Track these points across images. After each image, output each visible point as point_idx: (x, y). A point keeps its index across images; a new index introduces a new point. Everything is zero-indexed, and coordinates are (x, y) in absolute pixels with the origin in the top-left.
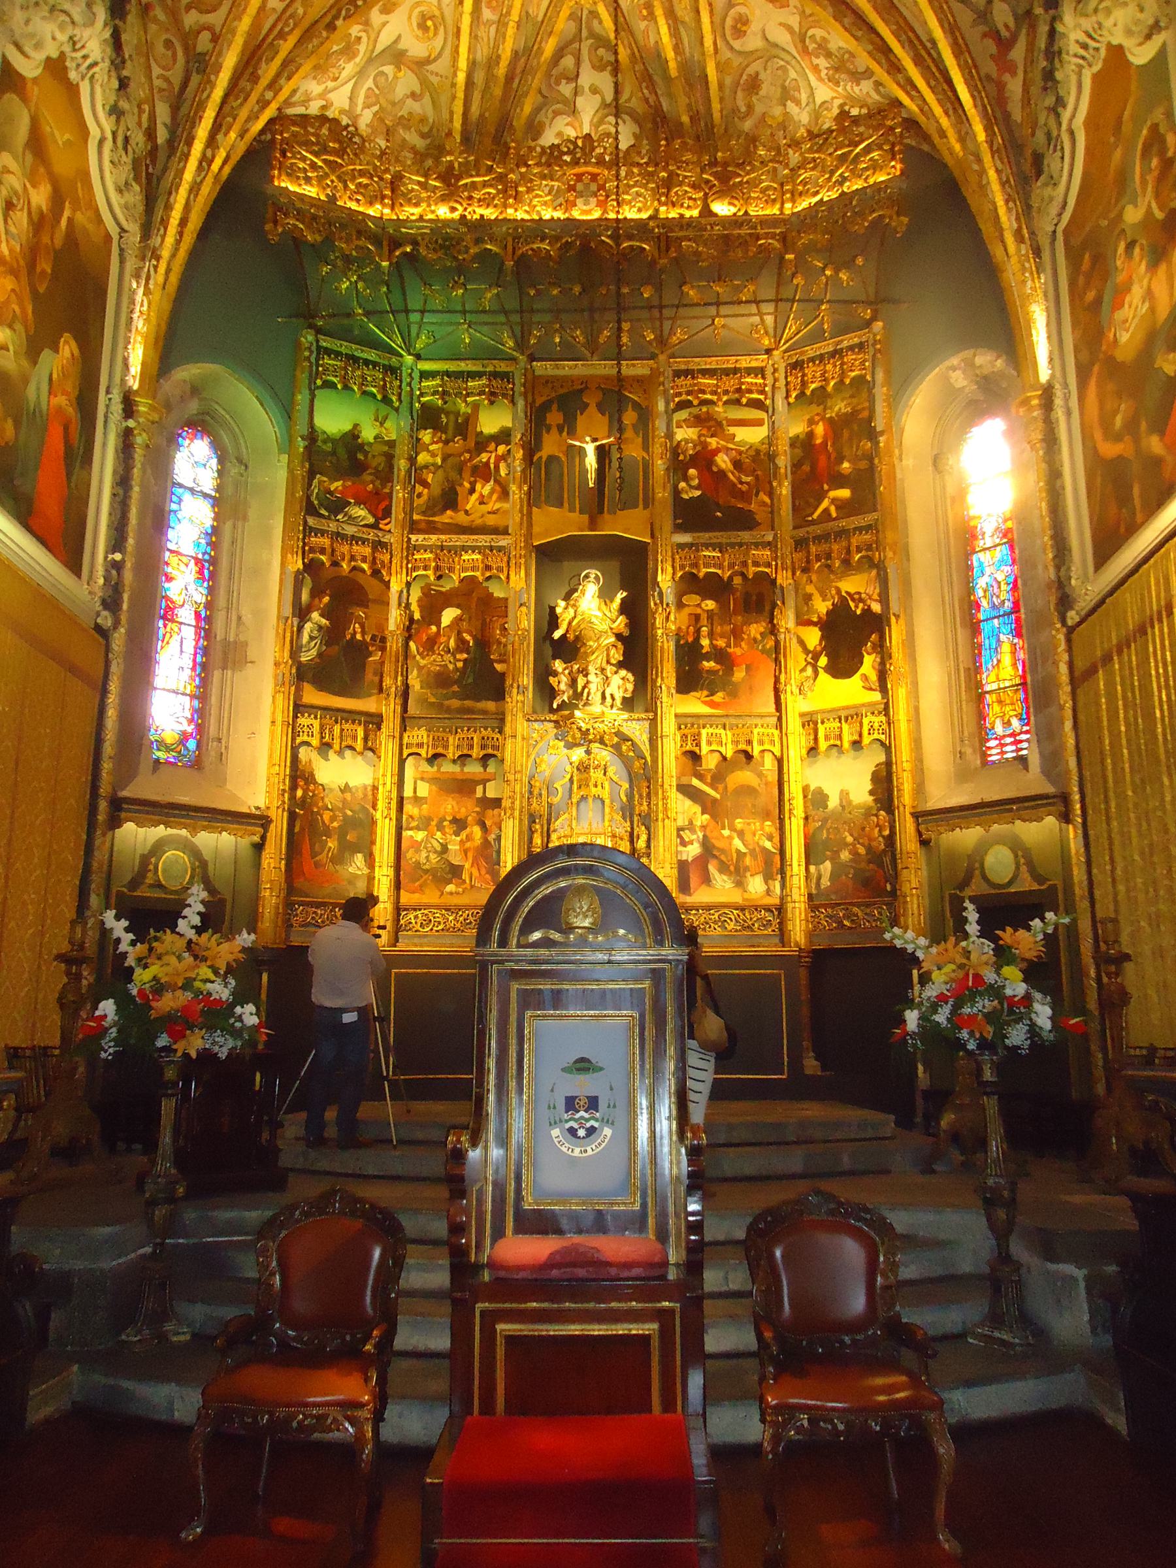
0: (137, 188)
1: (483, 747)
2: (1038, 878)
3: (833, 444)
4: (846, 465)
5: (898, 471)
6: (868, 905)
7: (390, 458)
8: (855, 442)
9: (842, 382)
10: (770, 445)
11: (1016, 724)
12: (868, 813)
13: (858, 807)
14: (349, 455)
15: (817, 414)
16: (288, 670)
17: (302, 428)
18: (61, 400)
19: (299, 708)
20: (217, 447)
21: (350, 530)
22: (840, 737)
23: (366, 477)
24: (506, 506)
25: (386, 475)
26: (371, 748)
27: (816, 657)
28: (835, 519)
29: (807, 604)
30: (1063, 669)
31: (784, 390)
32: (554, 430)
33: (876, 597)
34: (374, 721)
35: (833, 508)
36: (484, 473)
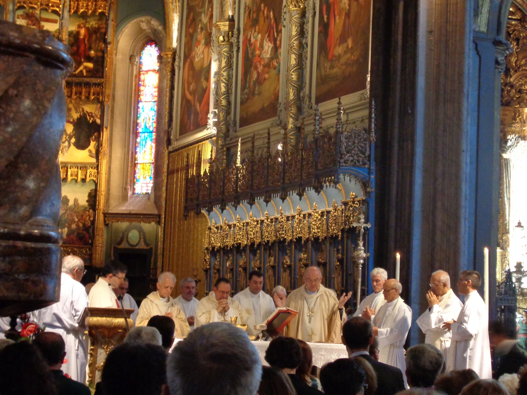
2: (147, 244)
3: (88, 41)
4: (92, 52)
5: (114, 60)
6: (82, 248)
8: (98, 42)
9: (94, 11)
10: (59, 33)
11: (148, 178)
12: (85, 210)
13: (82, 206)
15: (82, 24)
22: (77, 175)
27: (70, 138)
28: (86, 77)
29: (69, 113)
30: (165, 166)
31: (68, 7)
33: (99, 116)
35: (84, 71)
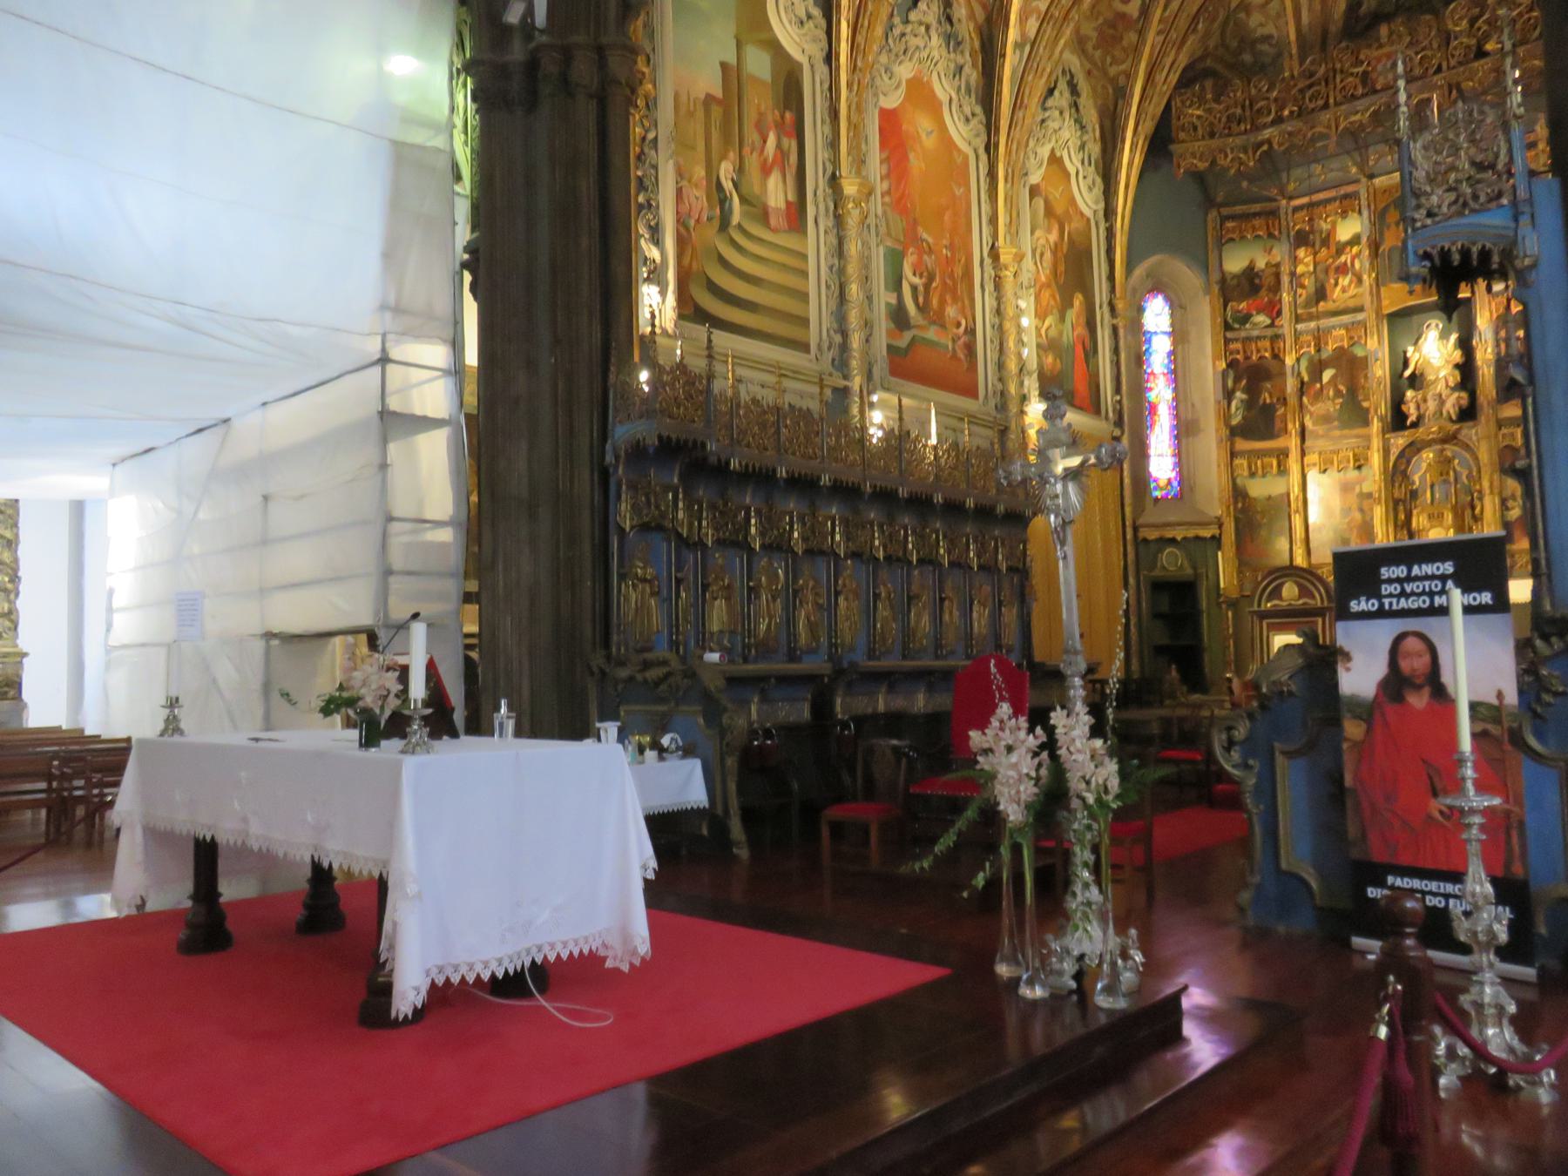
0: (1099, 180)
1: (1356, 460)
7: (1277, 276)
14: (1251, 282)
16: (1225, 432)
17: (1216, 276)
18: (1081, 330)
19: (1233, 455)
20: (1168, 299)
21: (1255, 333)
23: (1263, 292)
24: (1360, 290)
25: (1276, 288)
26: (1283, 471)
32: (1393, 227)
34: (1283, 454)
36: (1343, 270)
